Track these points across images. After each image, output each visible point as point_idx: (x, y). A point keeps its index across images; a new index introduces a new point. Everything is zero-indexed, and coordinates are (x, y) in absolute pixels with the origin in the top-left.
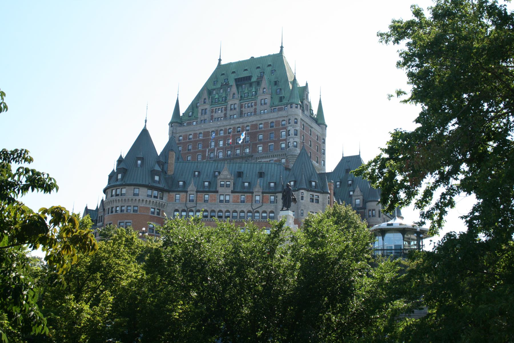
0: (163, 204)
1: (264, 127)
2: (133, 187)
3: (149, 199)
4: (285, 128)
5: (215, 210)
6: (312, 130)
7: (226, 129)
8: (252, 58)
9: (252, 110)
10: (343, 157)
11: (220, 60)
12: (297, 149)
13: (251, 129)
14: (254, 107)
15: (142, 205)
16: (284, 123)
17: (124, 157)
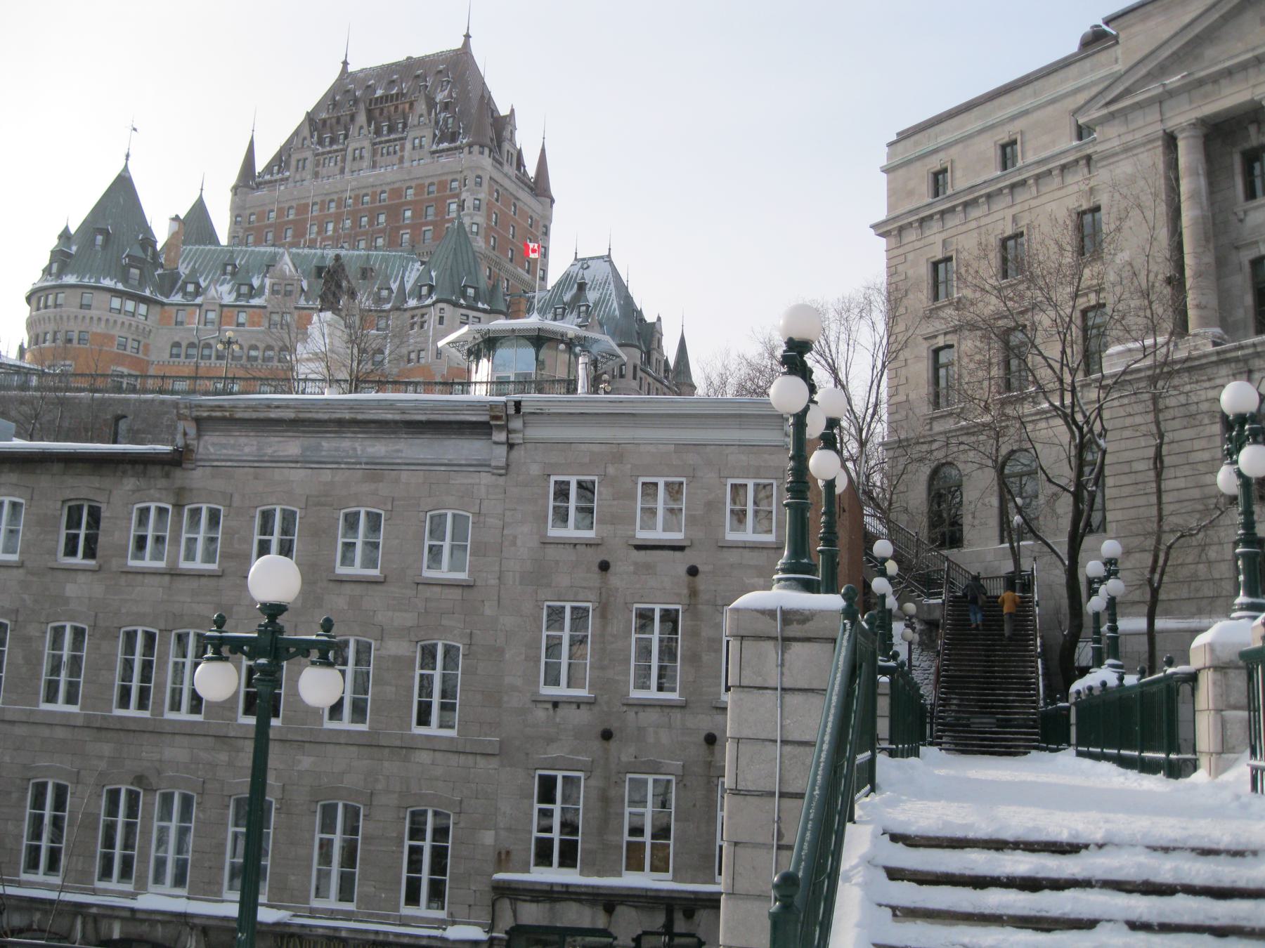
0: (147, 329)
1: (415, 195)
2: (79, 291)
3: (114, 316)
4: (458, 196)
5: (259, 344)
6: (519, 204)
7: (340, 199)
8: (409, 58)
9: (395, 159)
10: (576, 259)
11: (345, 63)
12: (478, 238)
13: (390, 198)
14: (399, 154)
15: (99, 330)
16: (455, 185)
17: (73, 230)
